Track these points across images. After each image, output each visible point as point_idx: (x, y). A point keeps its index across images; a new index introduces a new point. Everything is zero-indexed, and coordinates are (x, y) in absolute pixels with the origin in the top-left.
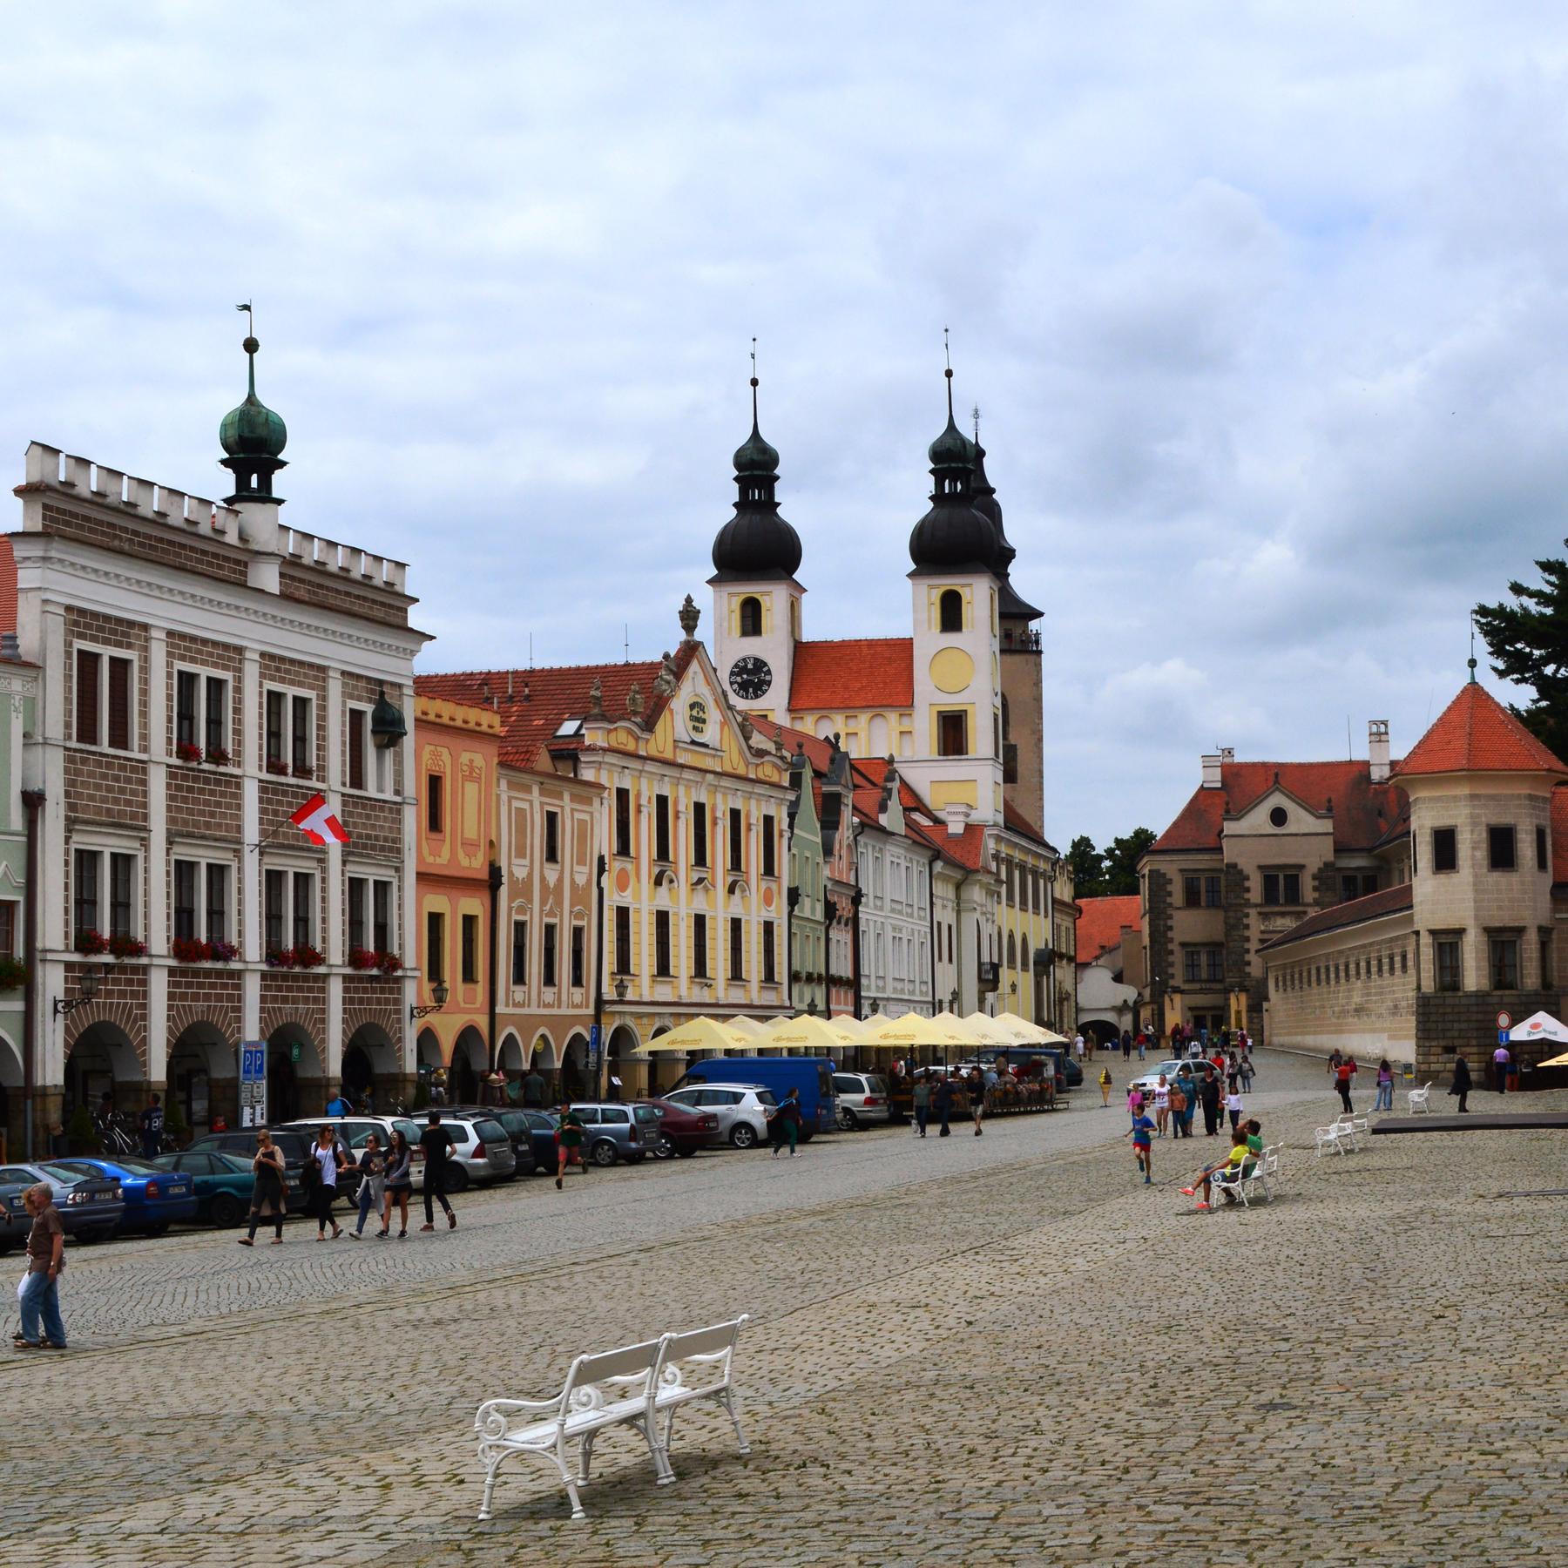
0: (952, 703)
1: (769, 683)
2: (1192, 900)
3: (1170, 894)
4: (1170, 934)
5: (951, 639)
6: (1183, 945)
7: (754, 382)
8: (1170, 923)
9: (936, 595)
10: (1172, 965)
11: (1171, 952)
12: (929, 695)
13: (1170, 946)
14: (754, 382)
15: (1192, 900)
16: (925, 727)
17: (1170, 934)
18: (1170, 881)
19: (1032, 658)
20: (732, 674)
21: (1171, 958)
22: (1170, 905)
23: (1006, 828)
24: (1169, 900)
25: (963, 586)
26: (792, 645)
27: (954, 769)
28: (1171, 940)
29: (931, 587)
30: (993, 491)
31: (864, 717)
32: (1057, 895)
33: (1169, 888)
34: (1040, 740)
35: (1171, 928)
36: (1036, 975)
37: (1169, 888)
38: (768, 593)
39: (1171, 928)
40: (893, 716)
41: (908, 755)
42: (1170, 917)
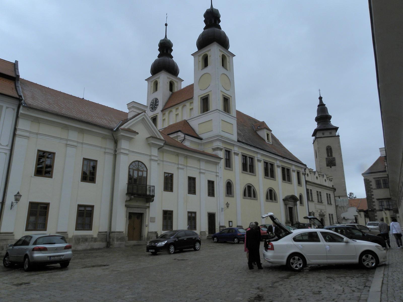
0: (203, 93)
1: (158, 105)
2: (379, 186)
3: (371, 185)
4: (373, 197)
5: (206, 70)
6: (378, 199)
7: (166, 25)
8: (372, 193)
9: (201, 58)
10: (375, 205)
11: (374, 202)
12: (198, 94)
13: (373, 200)
14: (166, 25)
15: (379, 186)
16: (197, 103)
17: (373, 197)
18: (371, 182)
19: (337, 138)
20: (151, 105)
21: (374, 204)
22: (372, 188)
23: (238, 141)
24: (371, 187)
25: (208, 51)
26: (168, 93)
27: (207, 117)
28: (374, 198)
29: (199, 56)
30: (325, 105)
31: (180, 107)
32: (308, 179)
33: (371, 183)
34: (341, 155)
35: (373, 195)
36: (286, 205)
37: (371, 183)
38: (159, 78)
39: (373, 195)
40: (188, 104)
41: (193, 116)
42: (372, 192)
